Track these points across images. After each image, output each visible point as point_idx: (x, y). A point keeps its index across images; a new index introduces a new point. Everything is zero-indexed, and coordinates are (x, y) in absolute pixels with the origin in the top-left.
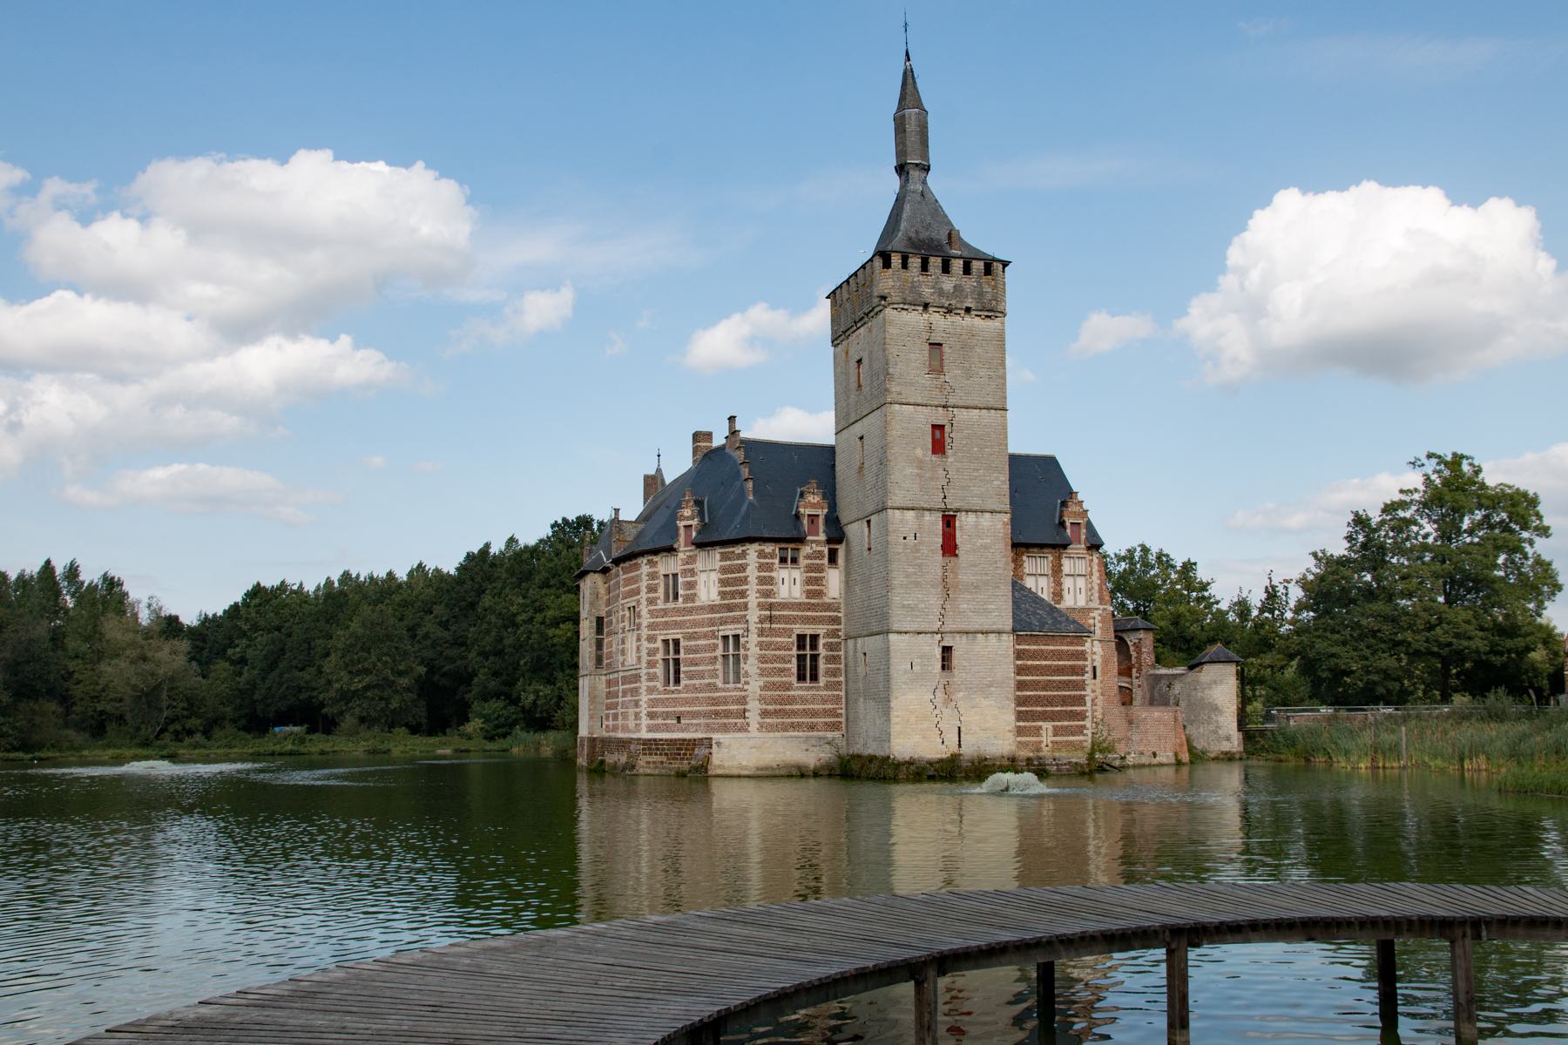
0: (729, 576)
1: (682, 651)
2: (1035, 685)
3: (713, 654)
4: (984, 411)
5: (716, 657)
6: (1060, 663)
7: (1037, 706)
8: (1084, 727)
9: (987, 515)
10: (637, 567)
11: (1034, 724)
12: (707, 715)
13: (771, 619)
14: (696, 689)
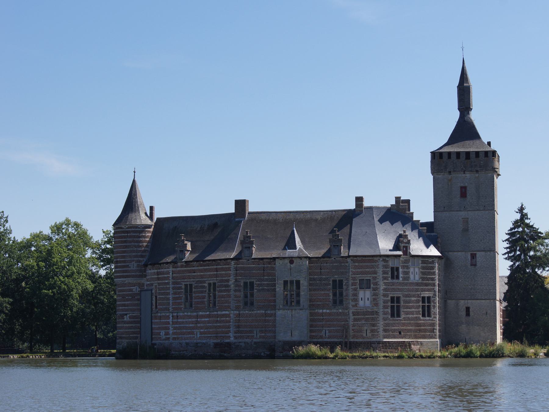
0: (426, 271)
3: (418, 304)
5: (419, 306)
10: (377, 261)
14: (409, 319)
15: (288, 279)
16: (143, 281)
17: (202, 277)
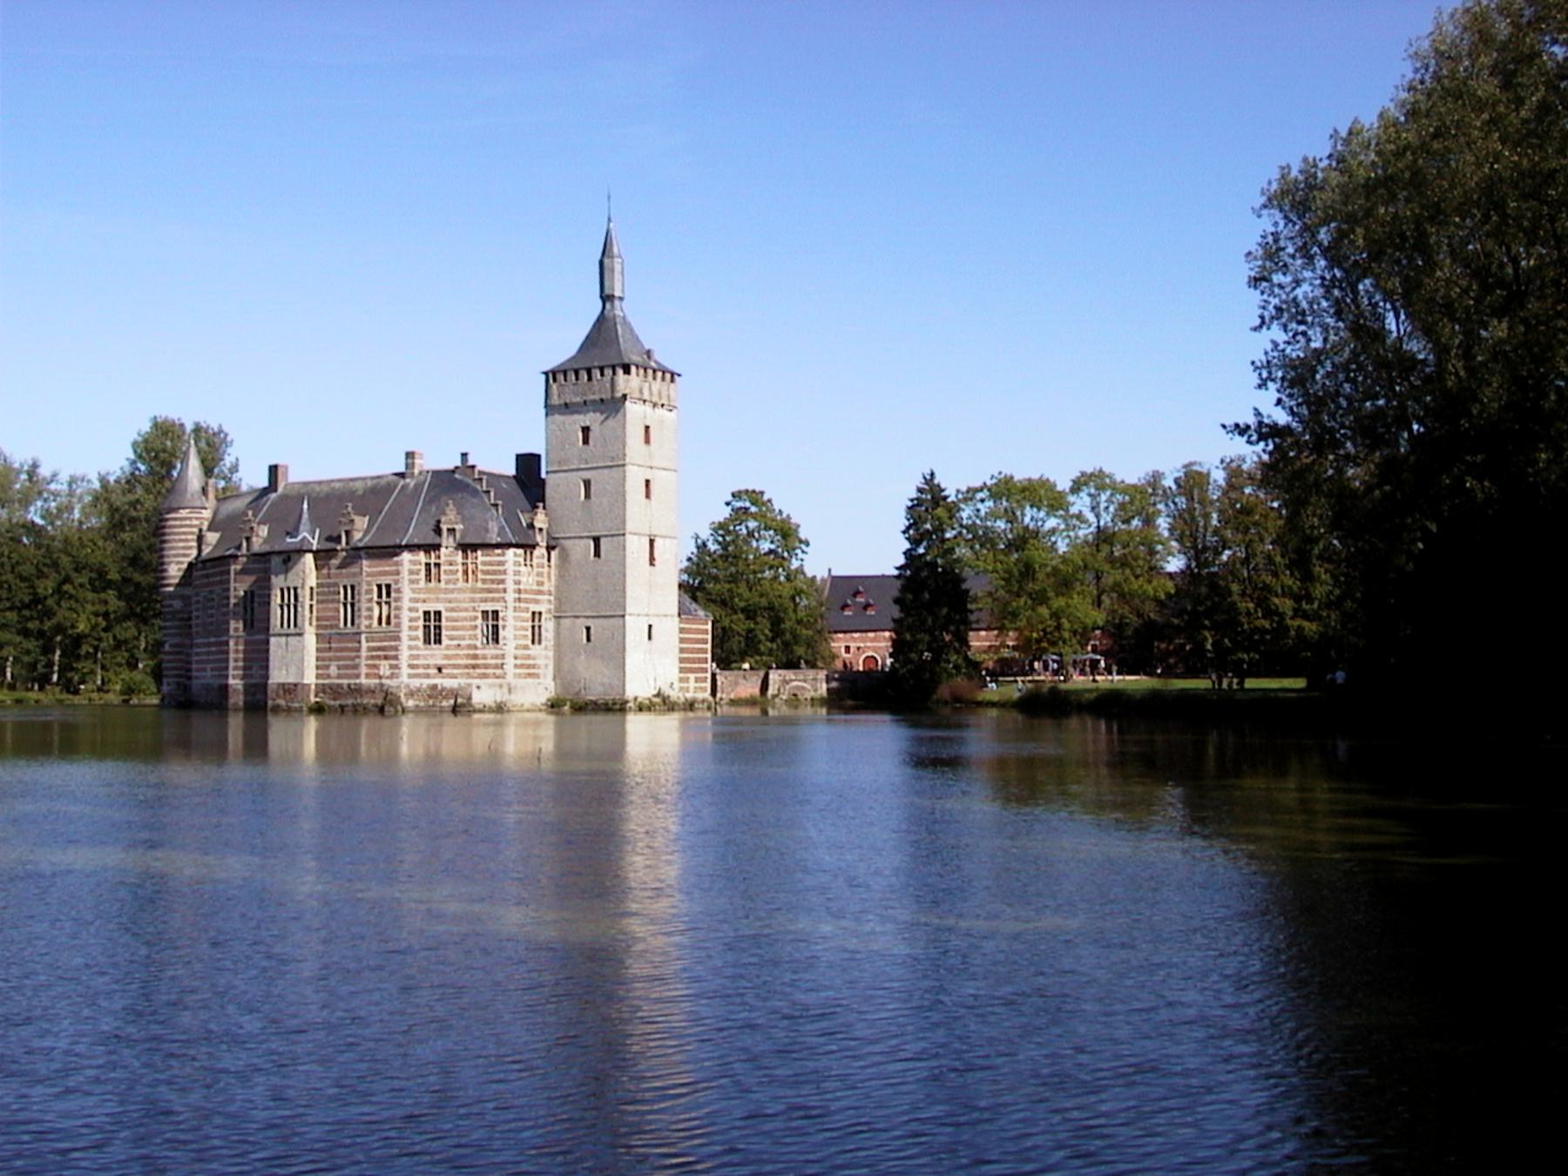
1: (443, 619)
2: (692, 651)
5: (476, 627)
10: (397, 555)
12: (466, 667)
13: (519, 600)
15: (284, 585)
16: (188, 591)
17: (213, 584)
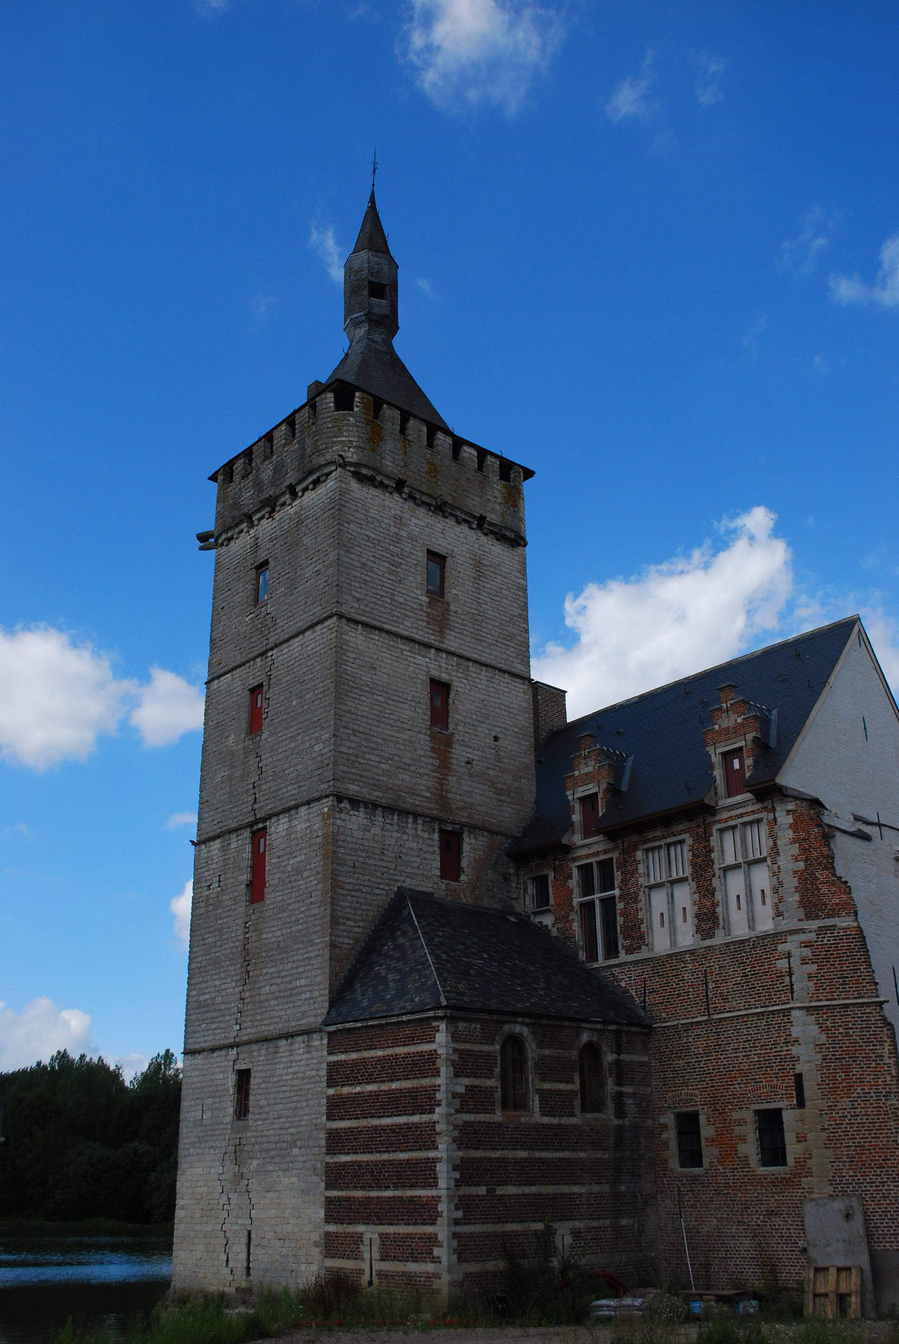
4: (307, 633)
6: (394, 1086)
7: (355, 1188)
8: (433, 1239)
9: (303, 810)
11: (351, 1229)
